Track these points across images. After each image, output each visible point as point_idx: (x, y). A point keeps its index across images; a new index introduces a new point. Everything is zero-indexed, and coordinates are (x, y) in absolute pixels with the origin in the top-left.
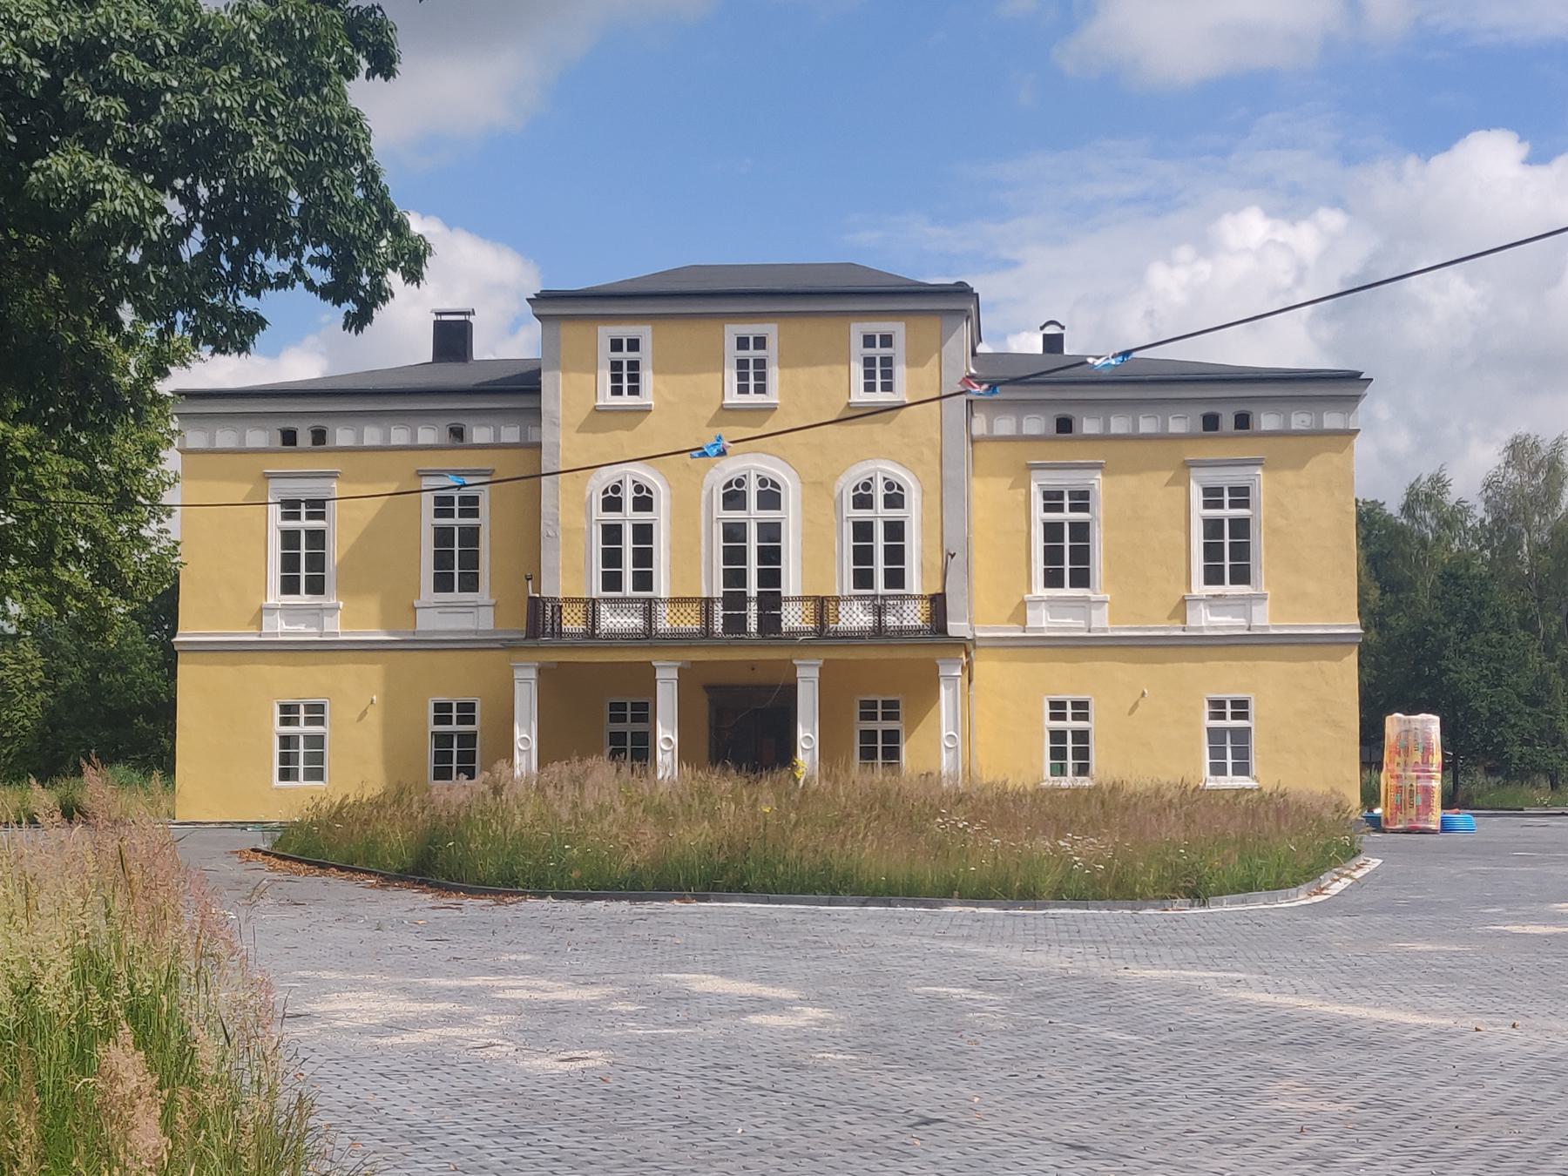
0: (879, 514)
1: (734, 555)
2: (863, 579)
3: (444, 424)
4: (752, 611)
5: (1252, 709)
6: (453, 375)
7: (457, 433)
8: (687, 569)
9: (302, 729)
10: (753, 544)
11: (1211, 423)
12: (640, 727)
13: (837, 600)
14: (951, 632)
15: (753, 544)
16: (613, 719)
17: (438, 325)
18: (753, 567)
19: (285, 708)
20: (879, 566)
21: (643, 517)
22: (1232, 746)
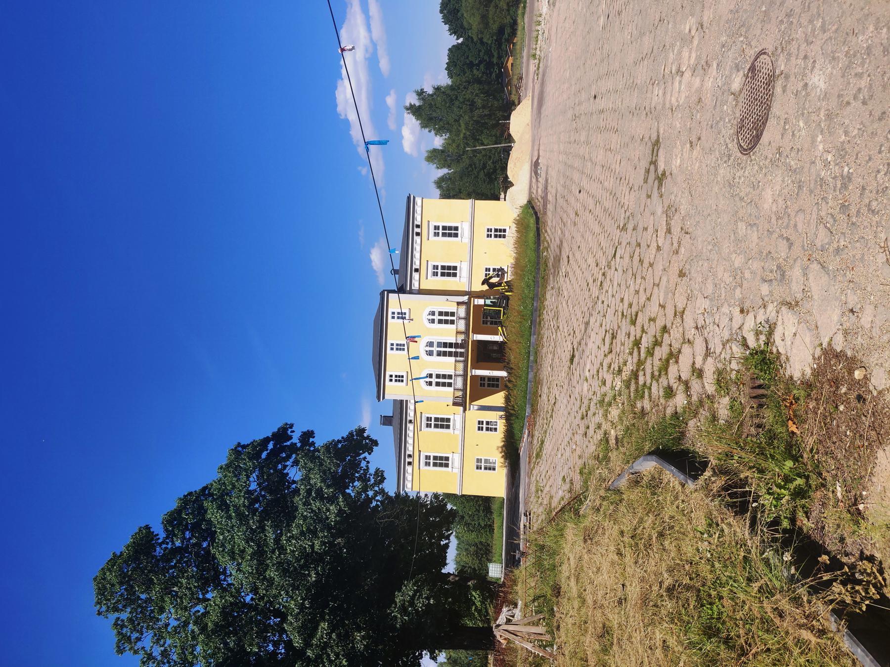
0: (437, 317)
1: (445, 354)
2: (452, 322)
4: (459, 350)
6: (396, 421)
7: (410, 421)
8: (448, 365)
9: (483, 465)
11: (418, 234)
17: (384, 424)
18: (448, 350)
19: (477, 468)
20: (449, 318)
22: (500, 233)
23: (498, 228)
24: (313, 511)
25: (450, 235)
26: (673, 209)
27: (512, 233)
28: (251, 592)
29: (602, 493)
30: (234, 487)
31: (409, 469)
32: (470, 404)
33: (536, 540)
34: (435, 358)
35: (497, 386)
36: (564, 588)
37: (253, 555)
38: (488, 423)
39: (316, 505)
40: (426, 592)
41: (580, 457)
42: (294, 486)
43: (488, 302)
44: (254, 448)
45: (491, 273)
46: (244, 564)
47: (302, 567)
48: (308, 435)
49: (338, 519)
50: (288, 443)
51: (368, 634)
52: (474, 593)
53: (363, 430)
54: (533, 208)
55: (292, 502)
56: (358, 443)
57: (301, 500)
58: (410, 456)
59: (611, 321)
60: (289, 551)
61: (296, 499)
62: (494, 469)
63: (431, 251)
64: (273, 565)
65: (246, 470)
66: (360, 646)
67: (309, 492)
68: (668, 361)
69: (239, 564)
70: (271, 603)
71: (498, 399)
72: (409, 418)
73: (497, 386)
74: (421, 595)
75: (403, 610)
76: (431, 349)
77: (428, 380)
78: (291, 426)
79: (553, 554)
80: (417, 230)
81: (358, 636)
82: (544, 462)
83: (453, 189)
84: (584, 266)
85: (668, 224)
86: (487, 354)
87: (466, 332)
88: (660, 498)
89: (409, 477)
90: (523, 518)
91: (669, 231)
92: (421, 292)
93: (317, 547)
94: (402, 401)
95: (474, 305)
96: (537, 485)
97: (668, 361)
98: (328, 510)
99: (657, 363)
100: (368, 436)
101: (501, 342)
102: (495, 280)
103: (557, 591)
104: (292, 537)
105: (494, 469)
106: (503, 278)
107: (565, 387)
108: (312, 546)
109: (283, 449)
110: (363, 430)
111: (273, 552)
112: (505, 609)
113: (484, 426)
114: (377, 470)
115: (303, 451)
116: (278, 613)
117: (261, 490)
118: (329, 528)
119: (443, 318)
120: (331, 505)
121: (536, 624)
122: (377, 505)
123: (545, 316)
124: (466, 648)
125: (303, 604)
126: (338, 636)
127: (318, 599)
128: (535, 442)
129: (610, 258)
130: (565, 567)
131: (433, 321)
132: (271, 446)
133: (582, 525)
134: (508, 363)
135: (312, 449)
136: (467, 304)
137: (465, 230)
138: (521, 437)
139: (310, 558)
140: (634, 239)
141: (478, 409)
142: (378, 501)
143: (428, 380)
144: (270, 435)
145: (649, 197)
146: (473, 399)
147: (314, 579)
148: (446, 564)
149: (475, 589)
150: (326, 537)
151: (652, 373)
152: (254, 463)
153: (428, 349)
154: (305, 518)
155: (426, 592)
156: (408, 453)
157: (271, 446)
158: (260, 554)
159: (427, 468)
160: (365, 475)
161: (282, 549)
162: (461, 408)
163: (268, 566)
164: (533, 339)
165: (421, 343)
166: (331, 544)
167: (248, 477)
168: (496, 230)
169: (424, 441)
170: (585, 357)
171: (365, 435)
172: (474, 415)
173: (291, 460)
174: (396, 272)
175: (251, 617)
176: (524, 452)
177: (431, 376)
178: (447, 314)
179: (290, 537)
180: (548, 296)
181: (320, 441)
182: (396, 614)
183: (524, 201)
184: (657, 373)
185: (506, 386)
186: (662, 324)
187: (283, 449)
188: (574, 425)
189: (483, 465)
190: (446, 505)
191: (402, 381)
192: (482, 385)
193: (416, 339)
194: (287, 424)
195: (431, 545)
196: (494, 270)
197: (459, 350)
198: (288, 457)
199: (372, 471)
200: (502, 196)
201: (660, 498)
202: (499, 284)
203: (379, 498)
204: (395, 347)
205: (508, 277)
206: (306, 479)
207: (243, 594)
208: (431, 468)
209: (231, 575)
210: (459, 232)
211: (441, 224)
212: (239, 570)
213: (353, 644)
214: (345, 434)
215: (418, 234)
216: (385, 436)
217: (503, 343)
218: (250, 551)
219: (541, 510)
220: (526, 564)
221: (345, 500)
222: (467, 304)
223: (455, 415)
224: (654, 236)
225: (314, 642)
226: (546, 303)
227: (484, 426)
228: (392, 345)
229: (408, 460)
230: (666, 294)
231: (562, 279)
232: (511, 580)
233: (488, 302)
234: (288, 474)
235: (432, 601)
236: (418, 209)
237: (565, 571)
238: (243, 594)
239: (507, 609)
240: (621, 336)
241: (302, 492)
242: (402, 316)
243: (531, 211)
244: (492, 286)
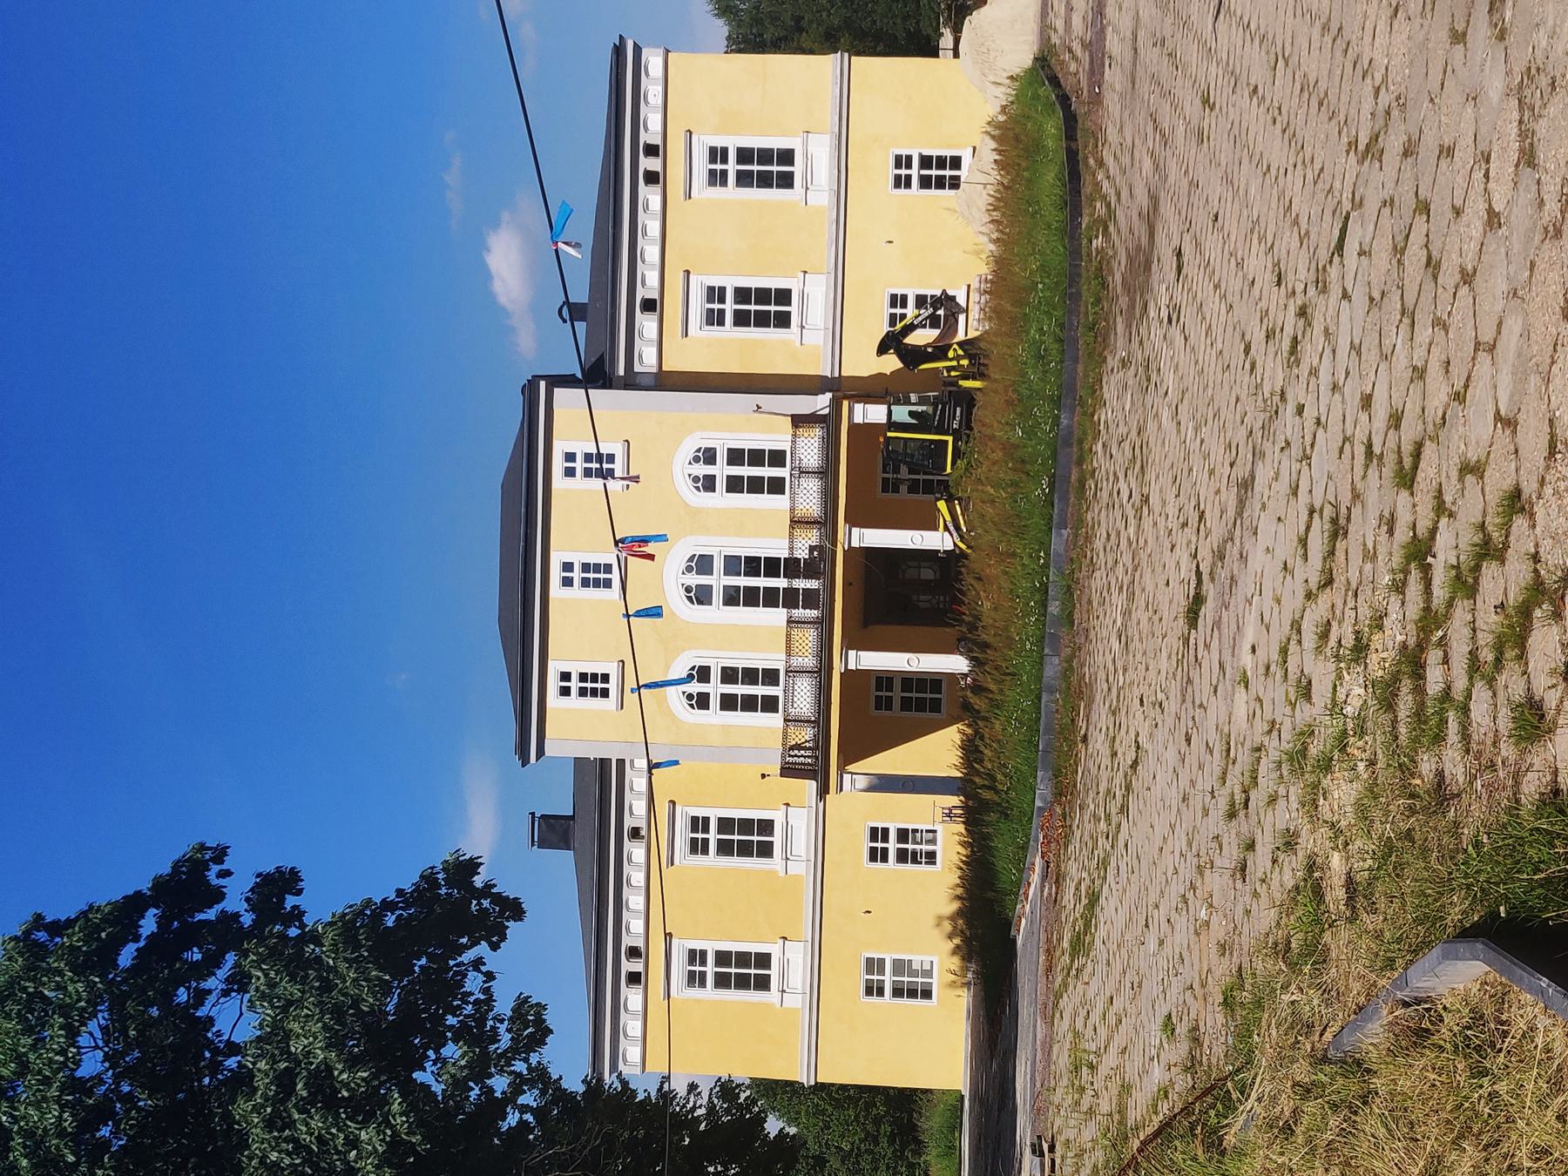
0: (722, 470)
1: (752, 597)
2: (777, 486)
3: (628, 844)
4: (801, 584)
5: (904, 152)
7: (635, 833)
9: (888, 979)
10: (743, 581)
11: (652, 178)
12: (897, 685)
13: (792, 509)
14: (826, 411)
15: (743, 581)
16: (889, 707)
18: (762, 582)
20: (767, 472)
21: (715, 675)
22: (939, 172)
23: (934, 152)
24: (299, 1147)
25: (765, 181)
26: (1544, 81)
27: (980, 169)
29: (1301, 1071)
30: (24, 1067)
31: (633, 997)
32: (841, 770)
34: (717, 613)
35: (936, 706)
38: (903, 835)
39: (310, 1126)
41: (1223, 949)
42: (232, 1062)
43: (901, 413)
44: (91, 931)
45: (911, 311)
48: (277, 886)
50: (211, 914)
53: (472, 866)
54: (1055, 81)
55: (227, 1117)
56: (457, 908)
58: (634, 952)
59: (1328, 474)
61: (242, 1107)
62: (927, 994)
63: (697, 237)
65: (65, 1010)
67: (285, 1082)
68: (1525, 612)
71: (938, 751)
72: (628, 823)
73: (936, 706)
76: (704, 580)
77: (695, 687)
78: (220, 854)
80: (647, 164)
82: (1101, 967)
83: (775, 18)
84: (1234, 284)
85: (1525, 134)
86: (895, 597)
87: (826, 523)
88: (1502, 1087)
89: (633, 1027)
91: (1528, 157)
92: (664, 381)
94: (604, 763)
95: (853, 427)
96: (1075, 1047)
97: (1525, 612)
98: (353, 1143)
99: (1489, 620)
100: (489, 886)
101: (950, 555)
102: (922, 337)
105: (927, 994)
106: (950, 326)
107: (1172, 706)
109: (194, 934)
110: (472, 866)
113: (892, 845)
114: (522, 1003)
115: (262, 940)
117: (117, 1078)
119: (746, 471)
120: (364, 1124)
122: (521, 1122)
123: (1100, 461)
128: (1068, 897)
129: (1323, 255)
131: (709, 484)
132: (149, 924)
134: (973, 627)
135: (293, 932)
136: (828, 422)
137: (816, 160)
138: (1020, 883)
140: (1406, 190)
141: (871, 789)
142: (524, 1109)
143: (695, 687)
144: (145, 886)
145: (1459, 37)
146: (851, 755)
151: (1473, 655)
152: (91, 986)
153: (695, 580)
156: (627, 942)
157: (149, 924)
159: (696, 992)
160: (481, 1021)
162: (811, 786)
164: (1058, 542)
165: (670, 560)
167: (72, 1033)
168: (926, 162)
169: (681, 900)
170: (1238, 600)
171: (478, 881)
172: (856, 806)
173: (223, 973)
174: (575, 312)
176: (1030, 933)
177: (703, 674)
178: (756, 457)
180: (1109, 391)
181: (320, 904)
183: (1020, 56)
184: (1487, 655)
185: (966, 706)
186: (1508, 484)
187: (194, 934)
188: (1203, 841)
189: (888, 979)
190: (760, 1120)
191: (605, 693)
192: (884, 704)
193: (649, 549)
194: (202, 847)
196: (921, 301)
197: (801, 584)
198: (211, 964)
199: (504, 1005)
200: (947, 40)
201: (1502, 1087)
202: (940, 351)
203: (528, 1098)
204: (577, 575)
205: (969, 327)
206: (275, 1037)
208: (710, 992)
210: (797, 169)
211: (732, 143)
214: (408, 882)
215: (652, 178)
216: (546, 884)
217: (953, 557)
219: (1090, 1132)
221: (411, 1108)
222: (828, 422)
223: (793, 811)
224: (1478, 175)
226: (1103, 415)
227: (892, 845)
228: (568, 567)
229: (628, 966)
230: (1520, 378)
231: (1157, 332)
233: (901, 413)
234: (210, 1021)
236: (652, 90)
240: (1364, 528)
241: (261, 1082)
242: (599, 465)
243: (1046, 91)
244: (913, 357)
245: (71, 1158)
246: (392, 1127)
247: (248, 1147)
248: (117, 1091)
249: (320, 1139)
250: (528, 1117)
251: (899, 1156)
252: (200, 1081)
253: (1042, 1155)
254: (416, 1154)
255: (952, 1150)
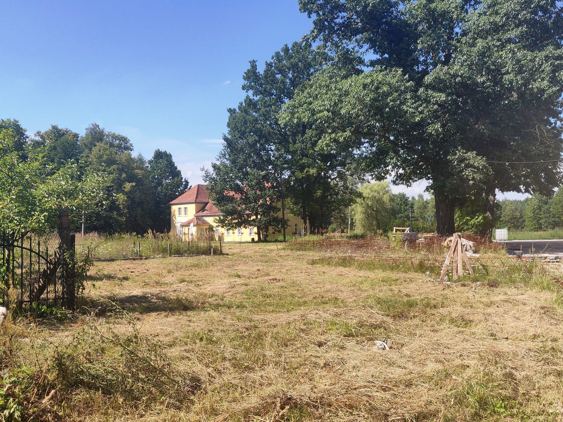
24: (540, 66)
28: (463, 31)
33: (536, 266)
36: (497, 290)
37: (495, 23)
39: (547, 67)
40: (478, 176)
46: (486, 17)
47: (488, 68)
49: (536, 90)
51: (440, 134)
52: (481, 217)
55: (548, 44)
57: (550, 52)
60: (501, 53)
61: (551, 48)
64: (487, 43)
66: (430, 129)
69: (485, 13)
70: (455, 50)
74: (475, 173)
75: (462, 160)
79: (526, 281)
81: (438, 126)
90: (553, 256)
93: (506, 77)
98: (543, 79)
103: (493, 285)
104: (514, 53)
108: (507, 73)
111: (499, 40)
112: (471, 243)
116: (448, 57)
117: (556, 13)
118: (526, 84)
120: (549, 81)
121: (464, 268)
122: (552, 124)
124: (437, 213)
125: (458, 76)
126: (436, 111)
127: (465, 88)
130: (514, 290)
133: (556, 306)
139: (496, 73)
142: (556, 123)
147: (479, 80)
148: (503, 192)
149: (484, 218)
150: (517, 82)
154: (533, 61)
155: (478, 176)
158: (496, 29)
161: (502, 47)
163: (486, 38)
166: (511, 89)
175: (443, 37)
179: (513, 51)
182: (458, 154)
190: (557, 186)
195: (519, 177)
207: (460, 24)
209: (475, 9)
212: (480, 14)
213: (431, 124)
218: (498, 19)
220: (512, 260)
221: (554, 93)
225: (430, 92)
232: (496, 247)
235: (471, 182)
237: (512, 291)
238: (460, 24)
239: (472, 245)
245: (532, 6)
246: (548, 89)
247: (539, 52)
248: (552, 13)
249: (544, 70)
250: (553, 125)
251: (550, 224)
252: (557, 35)
253: (555, 259)
254: (541, 96)
255: (553, 237)
